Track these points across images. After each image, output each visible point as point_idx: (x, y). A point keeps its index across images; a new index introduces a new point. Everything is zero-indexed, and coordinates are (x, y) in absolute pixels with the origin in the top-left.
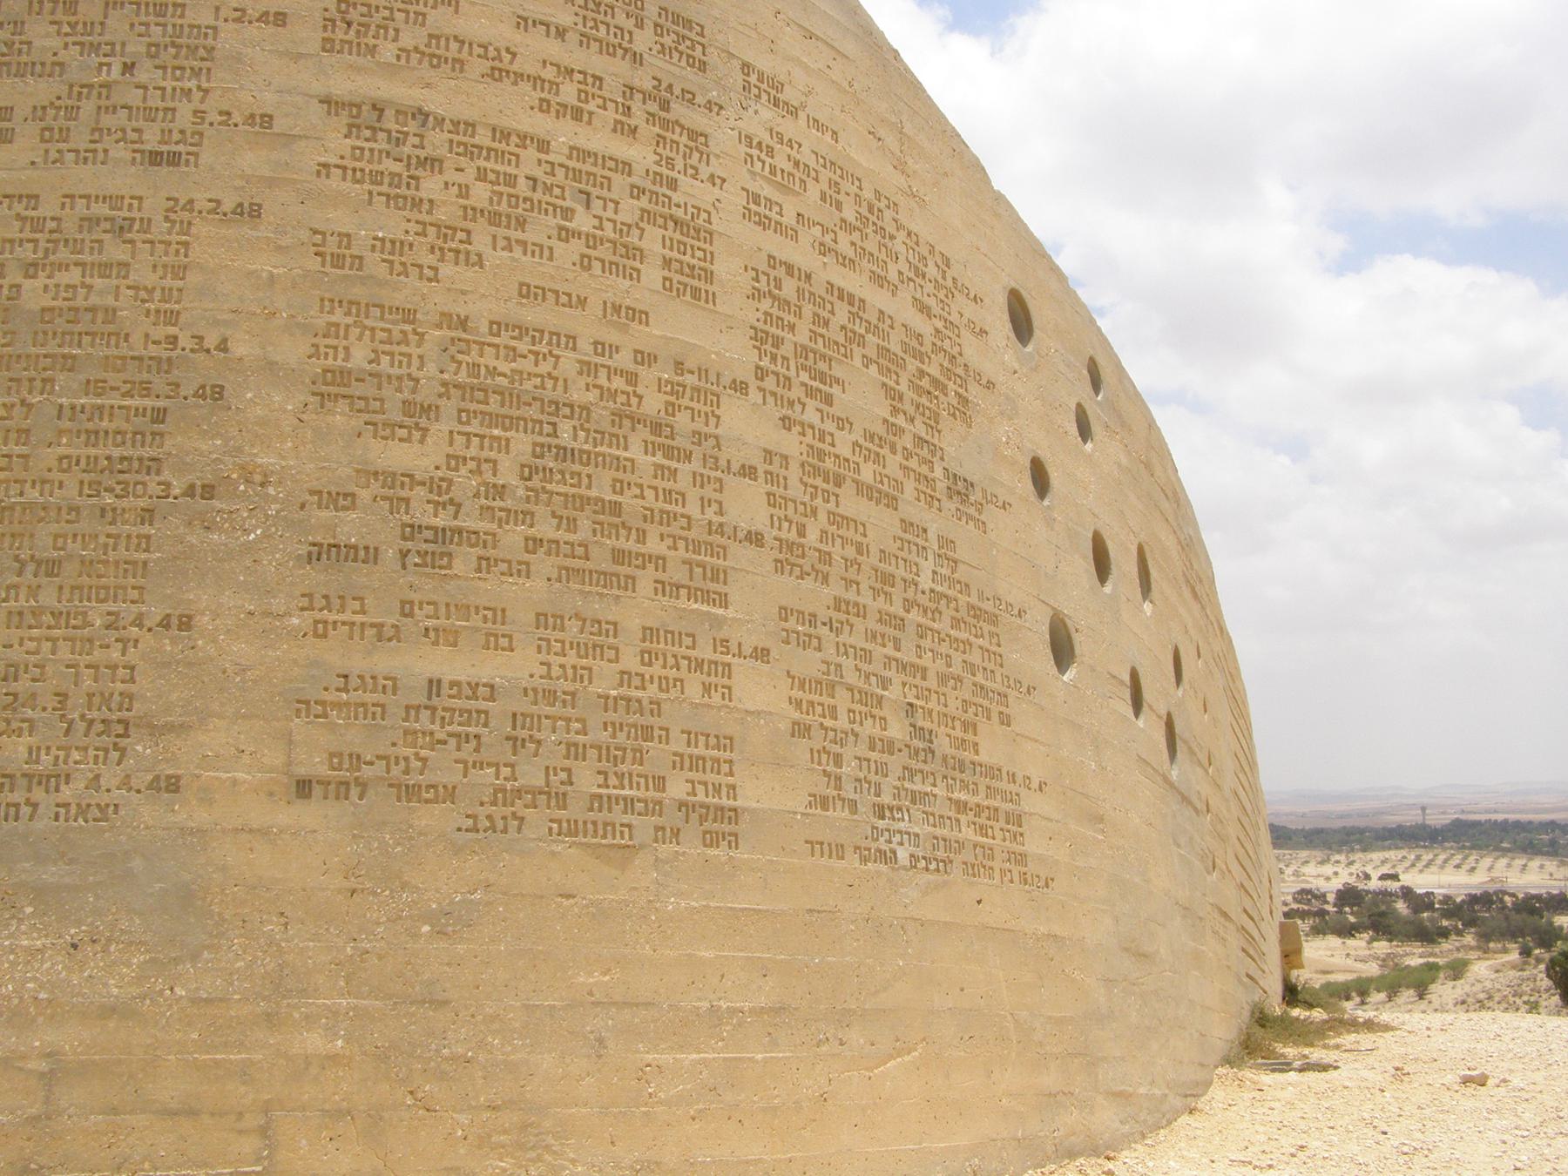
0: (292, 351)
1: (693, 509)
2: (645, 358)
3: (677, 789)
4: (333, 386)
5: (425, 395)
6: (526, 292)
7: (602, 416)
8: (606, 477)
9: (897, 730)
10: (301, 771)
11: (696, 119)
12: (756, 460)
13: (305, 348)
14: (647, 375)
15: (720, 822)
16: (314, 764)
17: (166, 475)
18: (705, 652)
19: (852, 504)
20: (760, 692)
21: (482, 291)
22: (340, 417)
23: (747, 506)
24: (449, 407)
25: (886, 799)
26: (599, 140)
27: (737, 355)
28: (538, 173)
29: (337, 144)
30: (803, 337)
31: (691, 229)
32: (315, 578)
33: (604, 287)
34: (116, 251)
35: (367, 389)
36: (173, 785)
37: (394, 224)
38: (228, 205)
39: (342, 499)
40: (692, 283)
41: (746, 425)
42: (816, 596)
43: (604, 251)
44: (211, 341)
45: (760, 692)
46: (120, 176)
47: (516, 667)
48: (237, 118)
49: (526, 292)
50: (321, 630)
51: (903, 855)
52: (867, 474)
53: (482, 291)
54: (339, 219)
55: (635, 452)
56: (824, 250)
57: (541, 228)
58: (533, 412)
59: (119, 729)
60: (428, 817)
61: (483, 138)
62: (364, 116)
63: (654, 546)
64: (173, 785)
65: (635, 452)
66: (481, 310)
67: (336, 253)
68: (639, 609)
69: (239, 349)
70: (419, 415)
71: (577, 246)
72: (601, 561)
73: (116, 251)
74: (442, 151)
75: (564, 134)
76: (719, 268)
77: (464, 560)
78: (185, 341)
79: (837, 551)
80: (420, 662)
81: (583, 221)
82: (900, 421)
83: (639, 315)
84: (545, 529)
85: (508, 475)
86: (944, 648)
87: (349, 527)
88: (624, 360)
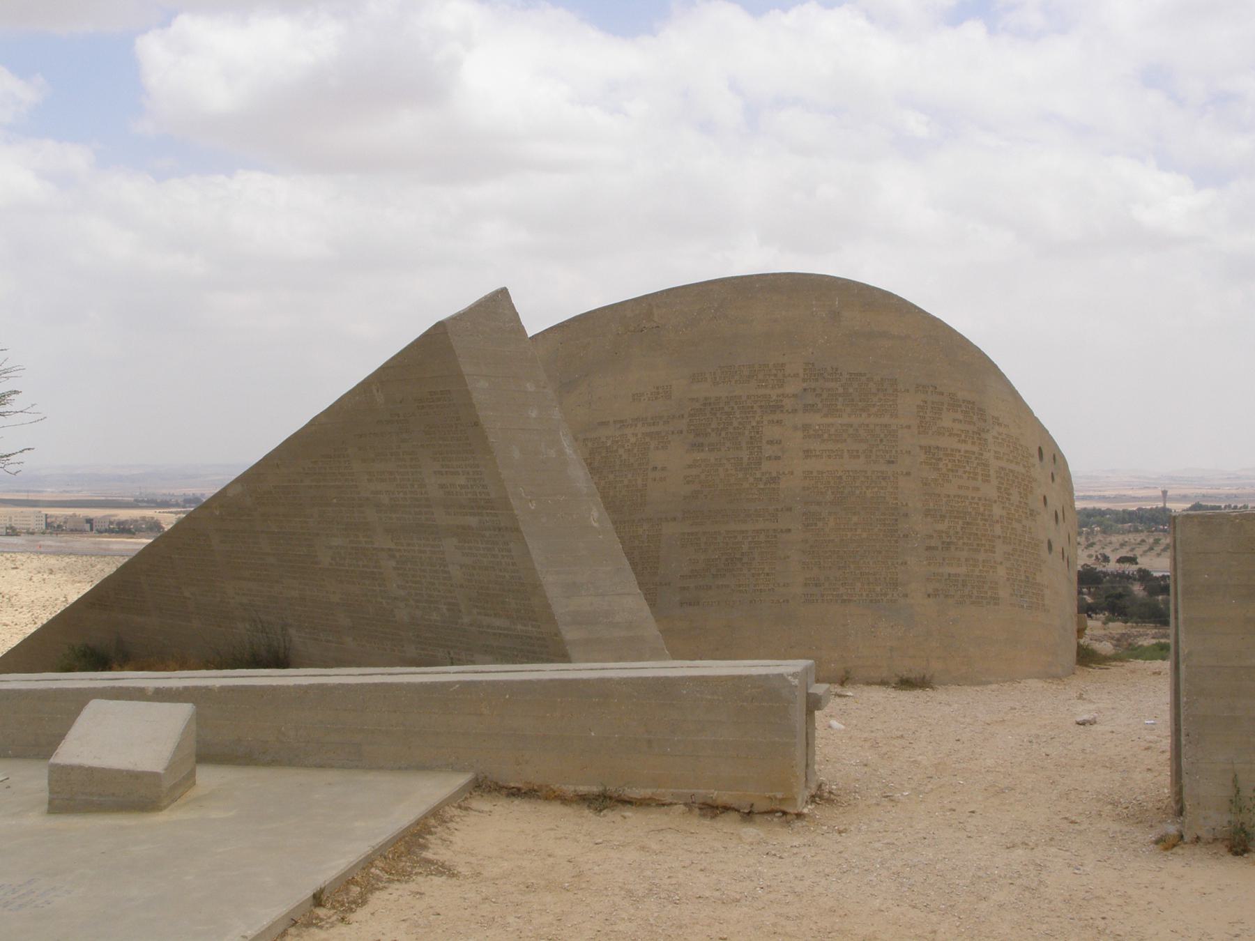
2: (980, 499)
4: (927, 513)
6: (960, 487)
19: (1015, 525)
20: (1002, 572)
23: (998, 530)
26: (969, 447)
34: (884, 484)
39: (931, 537)
40: (986, 480)
41: (997, 511)
45: (1002, 572)
47: (962, 570)
49: (960, 487)
50: (929, 564)
57: (960, 473)
62: (927, 449)
64: (906, 596)
70: (943, 517)
73: (884, 484)
75: (963, 447)
77: (953, 548)
80: (947, 570)
81: (968, 469)
83: (978, 489)
85: (959, 529)
87: (933, 543)
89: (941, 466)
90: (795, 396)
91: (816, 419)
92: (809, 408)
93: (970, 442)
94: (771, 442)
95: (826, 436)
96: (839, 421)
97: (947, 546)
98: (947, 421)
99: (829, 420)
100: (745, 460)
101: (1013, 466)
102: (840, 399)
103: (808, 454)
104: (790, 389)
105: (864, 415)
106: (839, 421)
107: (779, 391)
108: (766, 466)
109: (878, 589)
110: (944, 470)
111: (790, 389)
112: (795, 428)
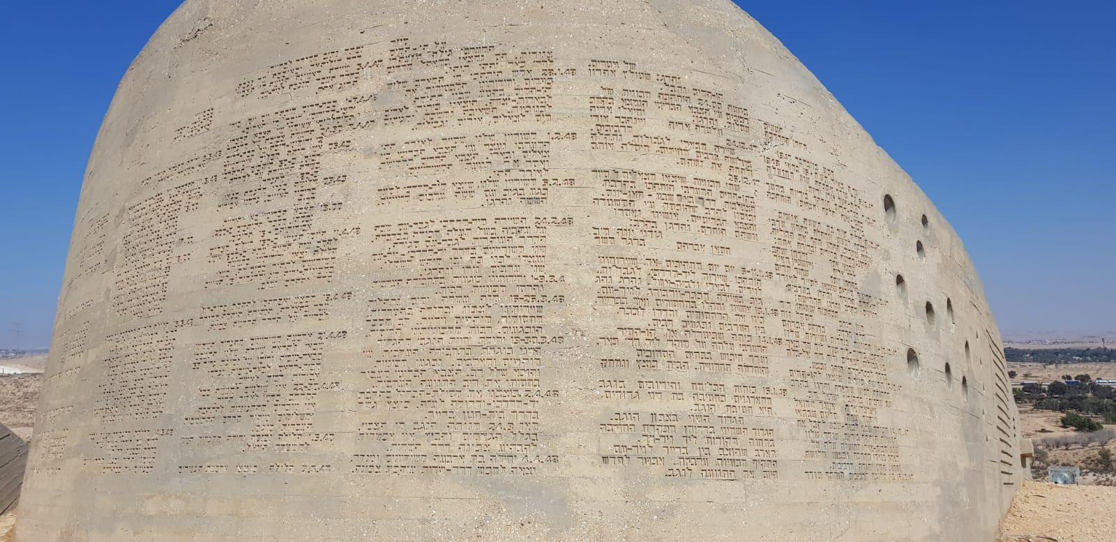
0: (589, 279)
1: (752, 332)
3: (752, 454)
5: (643, 293)
7: (713, 297)
8: (718, 320)
9: (842, 419)
10: (604, 454)
11: (746, 155)
12: (777, 306)
13: (594, 279)
14: (731, 276)
15: (769, 466)
16: (609, 450)
17: (544, 333)
18: (761, 393)
19: (818, 318)
21: (663, 247)
22: (610, 307)
24: (652, 298)
25: (839, 450)
26: (706, 171)
27: (767, 262)
28: (681, 192)
29: (600, 189)
30: (794, 246)
31: (746, 207)
32: (606, 374)
33: (708, 239)
35: (620, 293)
36: (554, 459)
37: (625, 221)
38: (559, 220)
40: (746, 230)
42: (805, 364)
43: (711, 224)
44: (557, 278)
45: (784, 408)
46: (516, 209)
47: (686, 405)
48: (560, 181)
51: (846, 473)
52: (824, 304)
53: (663, 247)
54: (602, 221)
55: (728, 309)
56: (803, 203)
57: (684, 217)
58: (687, 297)
59: (533, 438)
60: (656, 470)
61: (659, 179)
63: (737, 350)
65: (728, 309)
66: (663, 256)
67: (601, 235)
68: (732, 378)
69: (568, 280)
71: (700, 222)
72: (716, 357)
73: (517, 241)
74: (643, 188)
75: (690, 172)
76: (757, 221)
78: (547, 278)
79: (813, 340)
81: (701, 211)
82: (838, 275)
84: (693, 348)
85: (677, 324)
86: (860, 377)
88: (721, 270)
89: (639, 204)
90: (373, 97)
91: (402, 133)
92: (396, 115)
93: (708, 163)
94: (329, 180)
95: (417, 162)
96: (442, 132)
97: (647, 358)
98: (655, 122)
99: (426, 132)
100: (290, 215)
101: (816, 214)
102: (446, 94)
103: (386, 194)
104: (366, 87)
105: (487, 118)
106: (442, 132)
107: (349, 92)
108: (320, 221)
109: (495, 445)
110: (646, 215)
111: (365, 88)
112: (369, 152)
